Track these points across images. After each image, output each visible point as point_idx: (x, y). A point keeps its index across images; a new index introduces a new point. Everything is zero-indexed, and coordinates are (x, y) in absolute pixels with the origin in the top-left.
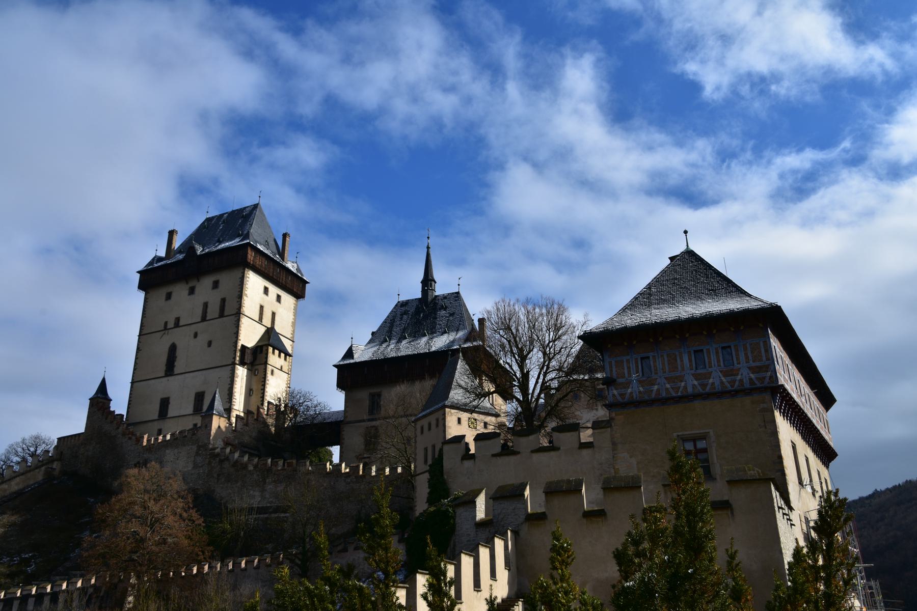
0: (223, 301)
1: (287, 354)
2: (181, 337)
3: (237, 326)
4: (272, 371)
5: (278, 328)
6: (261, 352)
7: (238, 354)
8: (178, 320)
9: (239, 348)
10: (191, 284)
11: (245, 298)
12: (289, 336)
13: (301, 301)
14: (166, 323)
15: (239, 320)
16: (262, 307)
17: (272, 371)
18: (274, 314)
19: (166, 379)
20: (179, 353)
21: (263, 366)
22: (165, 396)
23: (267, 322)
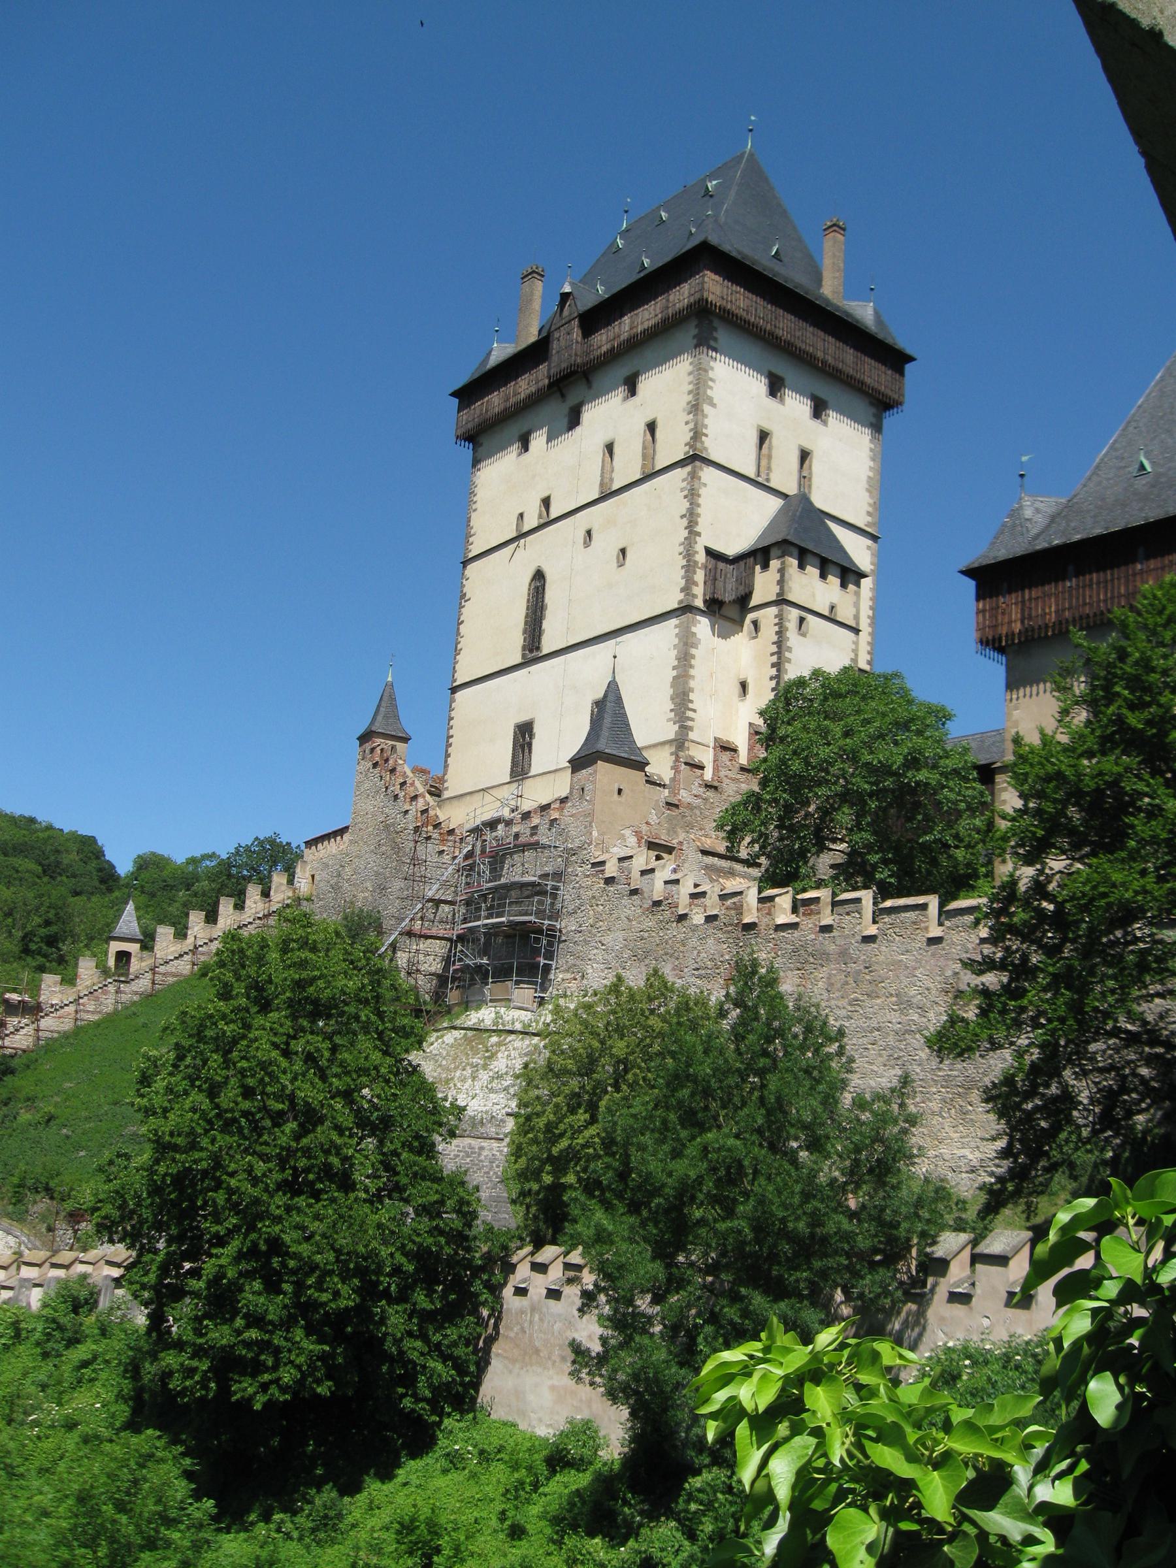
0: (651, 427)
1: (849, 575)
2: (552, 551)
3: (692, 495)
4: (802, 620)
5: (819, 500)
6: (765, 566)
7: (700, 576)
8: (546, 502)
9: (701, 557)
10: (572, 400)
11: (707, 408)
12: (861, 521)
13: (891, 420)
14: (521, 515)
15: (693, 476)
16: (763, 436)
17: (802, 620)
18: (804, 455)
19: (524, 671)
20: (552, 596)
21: (773, 611)
22: (523, 718)
23: (785, 478)
